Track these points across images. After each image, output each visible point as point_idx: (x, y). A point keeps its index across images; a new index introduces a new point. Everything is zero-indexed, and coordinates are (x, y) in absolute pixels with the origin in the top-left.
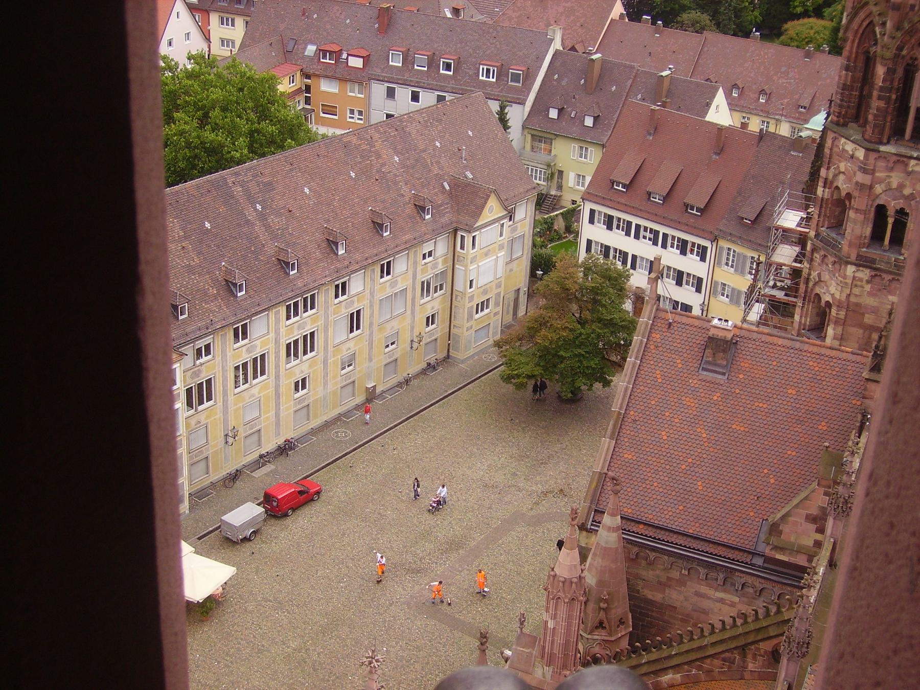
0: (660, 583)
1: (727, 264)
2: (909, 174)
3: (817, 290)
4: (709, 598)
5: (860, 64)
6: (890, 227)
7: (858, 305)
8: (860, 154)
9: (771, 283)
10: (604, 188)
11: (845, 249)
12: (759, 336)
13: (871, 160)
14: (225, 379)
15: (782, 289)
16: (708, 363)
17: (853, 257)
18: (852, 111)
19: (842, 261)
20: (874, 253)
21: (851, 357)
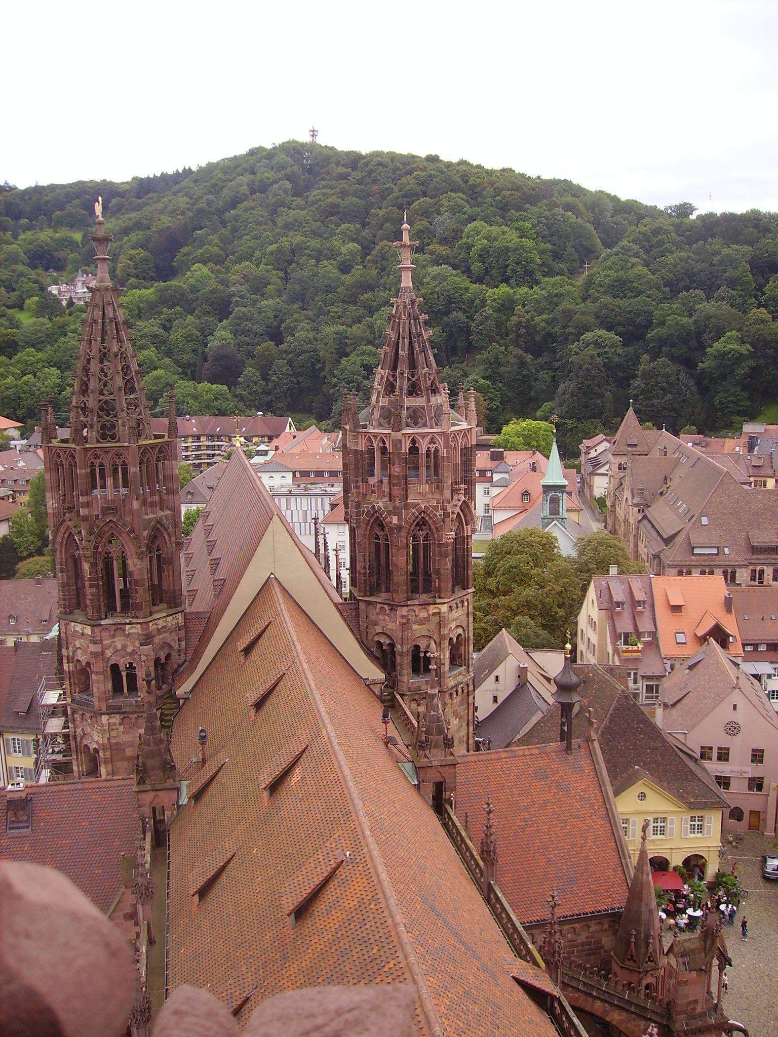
1: (15, 751)
2: (127, 636)
3: (85, 742)
5: (71, 566)
6: (124, 679)
7: (118, 744)
8: (88, 631)
9: (50, 751)
11: (97, 704)
12: (48, 789)
13: (98, 634)
15: (59, 752)
16: (13, 822)
17: (104, 709)
19: (97, 714)
20: (118, 701)
21: (122, 782)
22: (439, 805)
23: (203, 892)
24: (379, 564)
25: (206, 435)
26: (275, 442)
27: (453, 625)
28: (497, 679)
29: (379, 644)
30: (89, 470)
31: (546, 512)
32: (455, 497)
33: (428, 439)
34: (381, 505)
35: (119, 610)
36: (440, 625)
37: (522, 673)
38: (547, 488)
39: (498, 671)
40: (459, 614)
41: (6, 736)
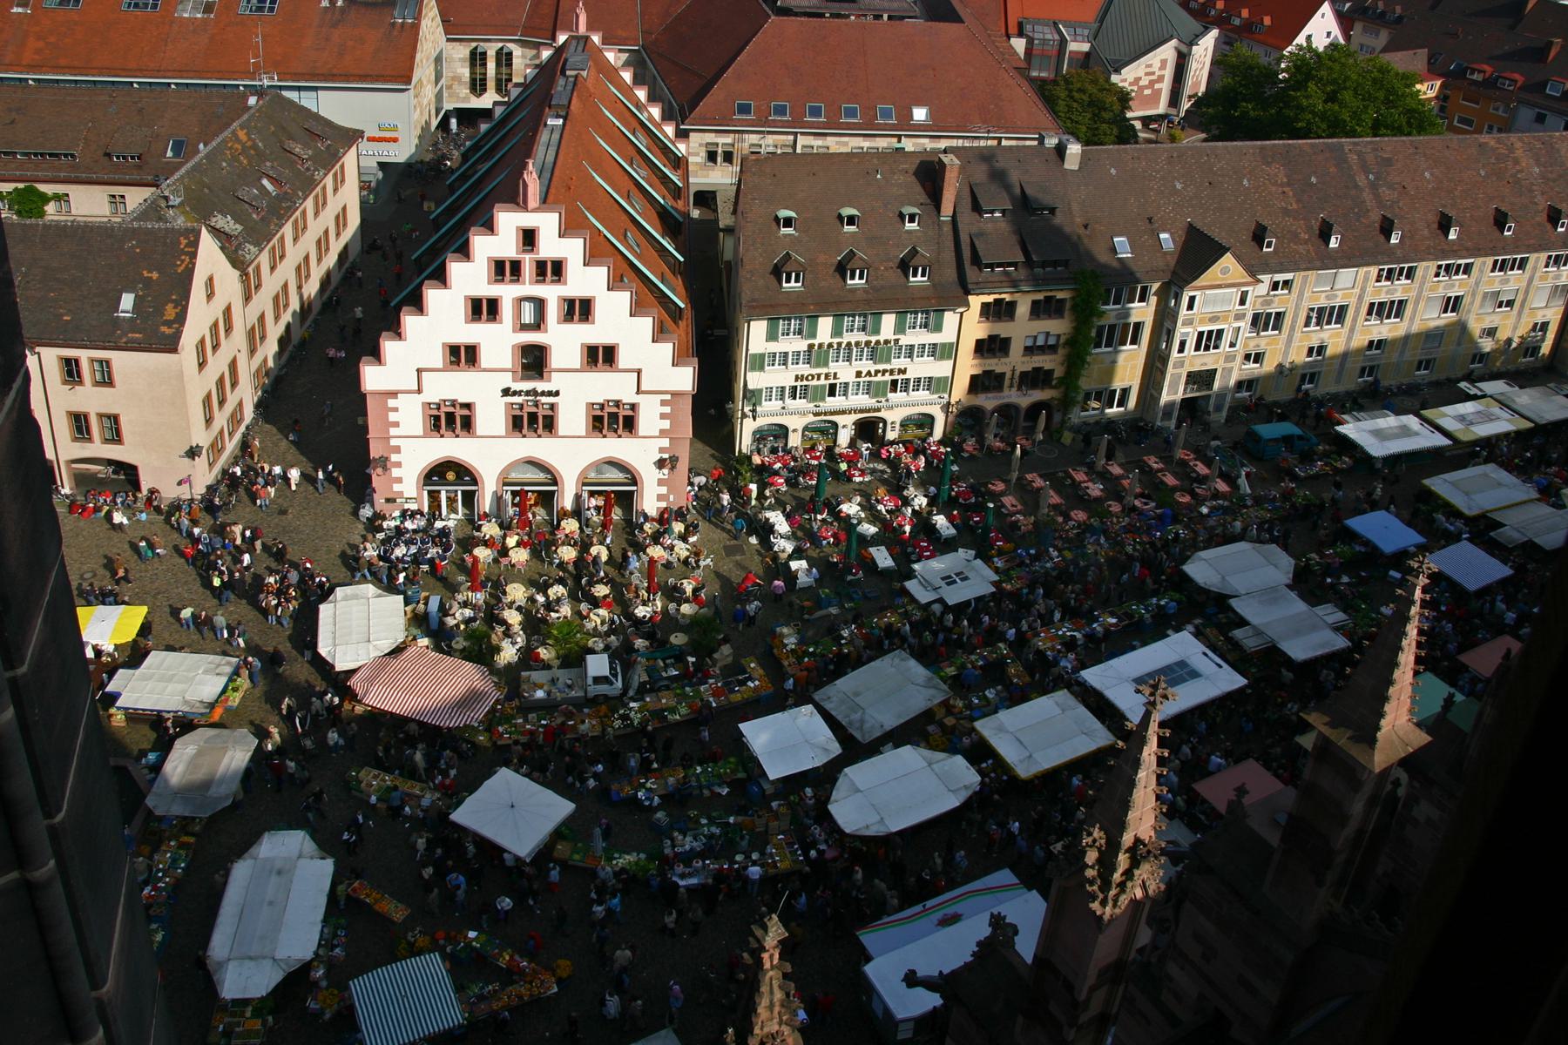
14: (1296, 316)
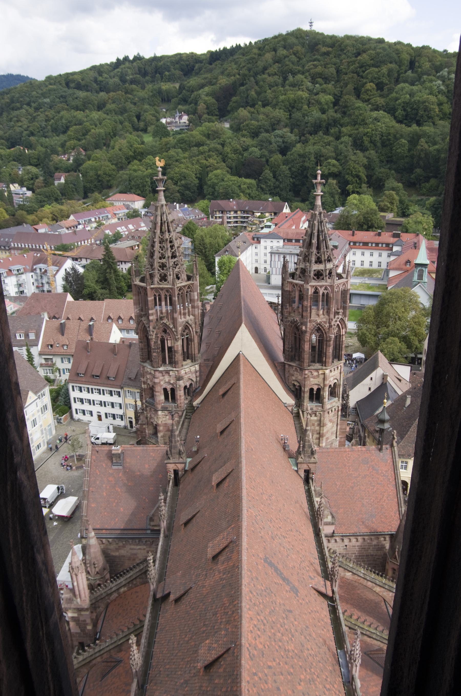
0: (116, 549)
3: (152, 421)
4: (135, 549)
5: (145, 340)
10: (76, 376)
18: (147, 357)
20: (167, 405)
22: (307, 480)
23: (186, 524)
24: (296, 346)
25: (241, 211)
26: (276, 219)
27: (332, 379)
28: (371, 379)
29: (294, 385)
30: (153, 298)
31: (415, 278)
32: (337, 317)
33: (323, 288)
34: (298, 319)
35: (167, 362)
36: (324, 379)
37: (384, 377)
38: (418, 265)
39: (373, 375)
40: (336, 373)
41: (125, 389)
